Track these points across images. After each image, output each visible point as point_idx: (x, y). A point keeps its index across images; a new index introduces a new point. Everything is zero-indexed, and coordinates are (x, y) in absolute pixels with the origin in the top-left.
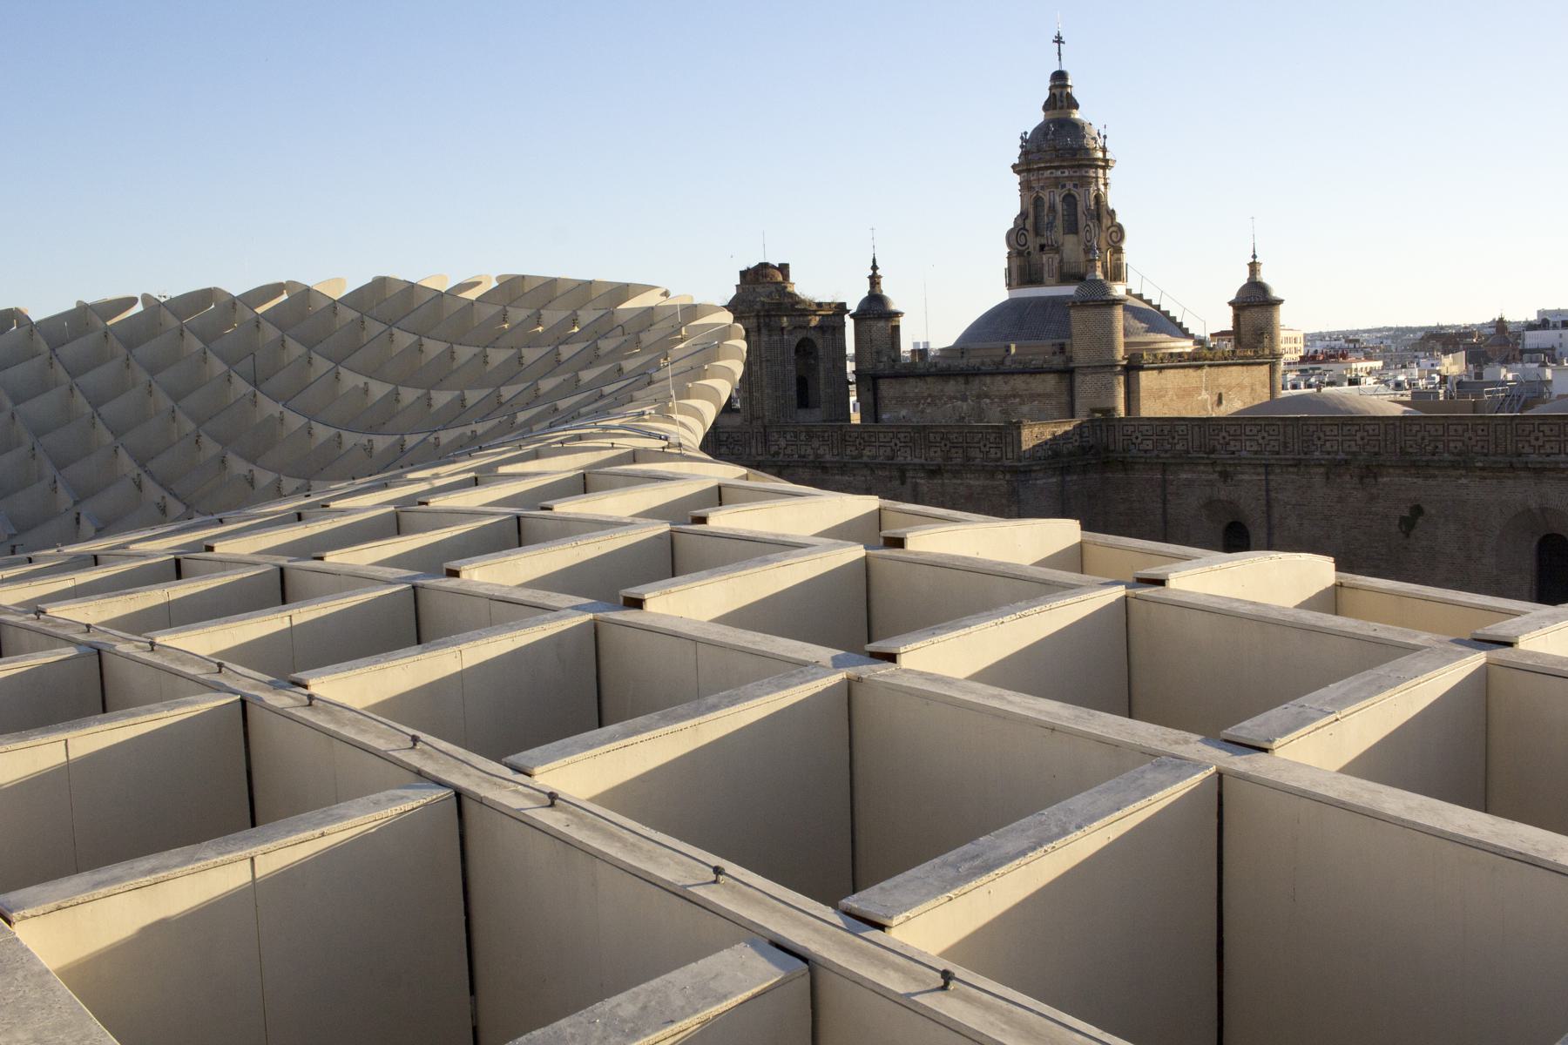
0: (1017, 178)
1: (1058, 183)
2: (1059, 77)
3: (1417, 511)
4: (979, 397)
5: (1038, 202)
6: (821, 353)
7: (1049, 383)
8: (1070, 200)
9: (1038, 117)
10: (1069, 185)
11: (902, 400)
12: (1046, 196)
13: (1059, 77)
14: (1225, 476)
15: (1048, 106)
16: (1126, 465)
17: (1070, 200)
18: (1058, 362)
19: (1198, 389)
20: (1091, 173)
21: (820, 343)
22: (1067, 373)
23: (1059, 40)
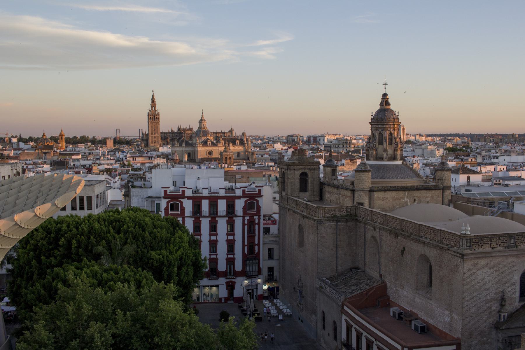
0: (370, 126)
1: (377, 129)
2: (385, 96)
3: (404, 248)
4: (340, 194)
5: (373, 134)
6: (309, 176)
7: (349, 193)
8: (380, 134)
9: (378, 107)
10: (380, 130)
11: (328, 192)
12: (374, 132)
13: (385, 96)
14: (375, 229)
15: (381, 104)
16: (360, 222)
17: (380, 134)
18: (351, 187)
19: (403, 198)
20: (387, 126)
21: (309, 174)
22: (353, 191)
23: (385, 84)
